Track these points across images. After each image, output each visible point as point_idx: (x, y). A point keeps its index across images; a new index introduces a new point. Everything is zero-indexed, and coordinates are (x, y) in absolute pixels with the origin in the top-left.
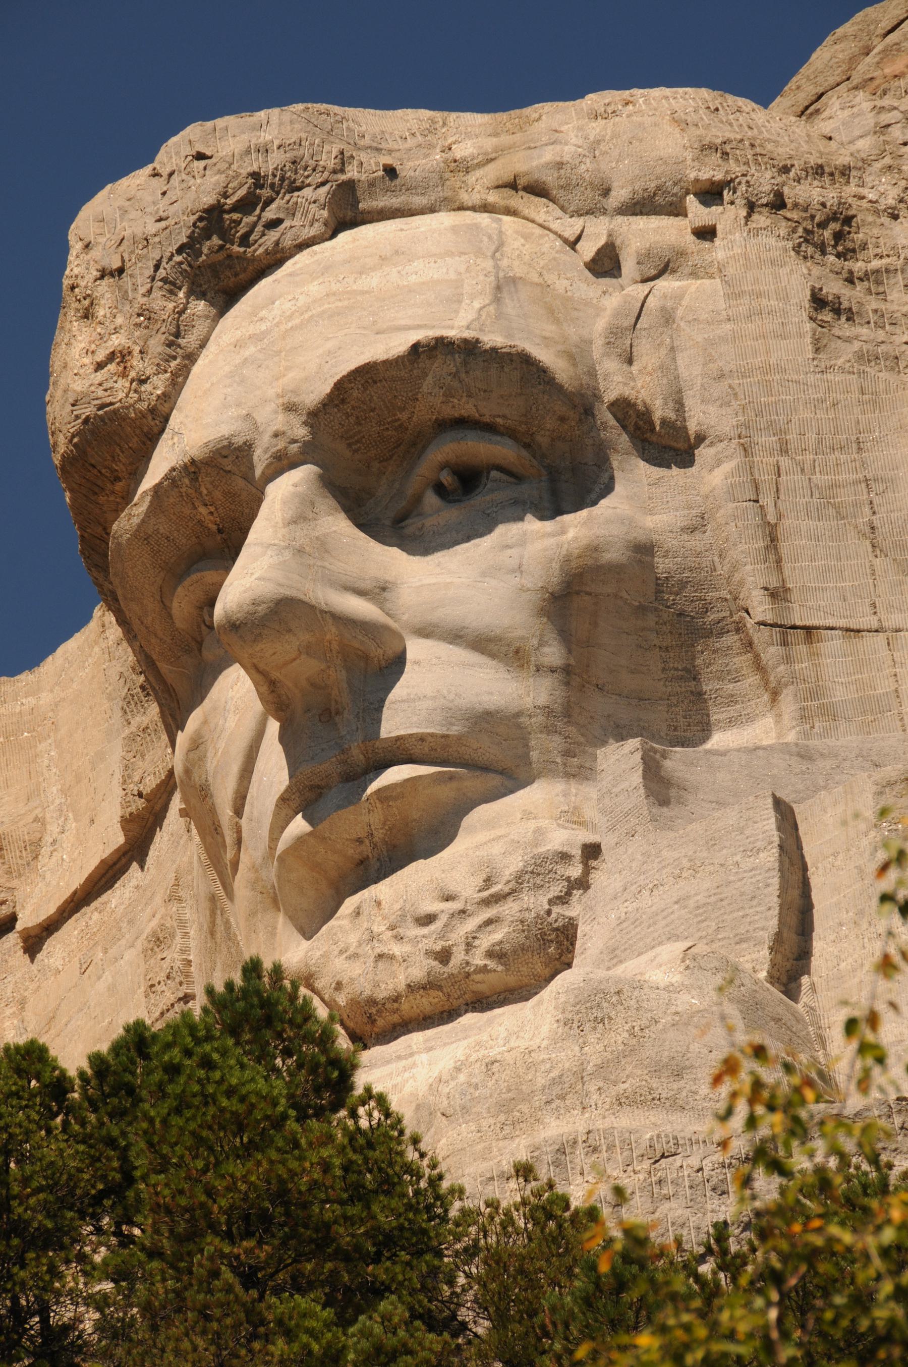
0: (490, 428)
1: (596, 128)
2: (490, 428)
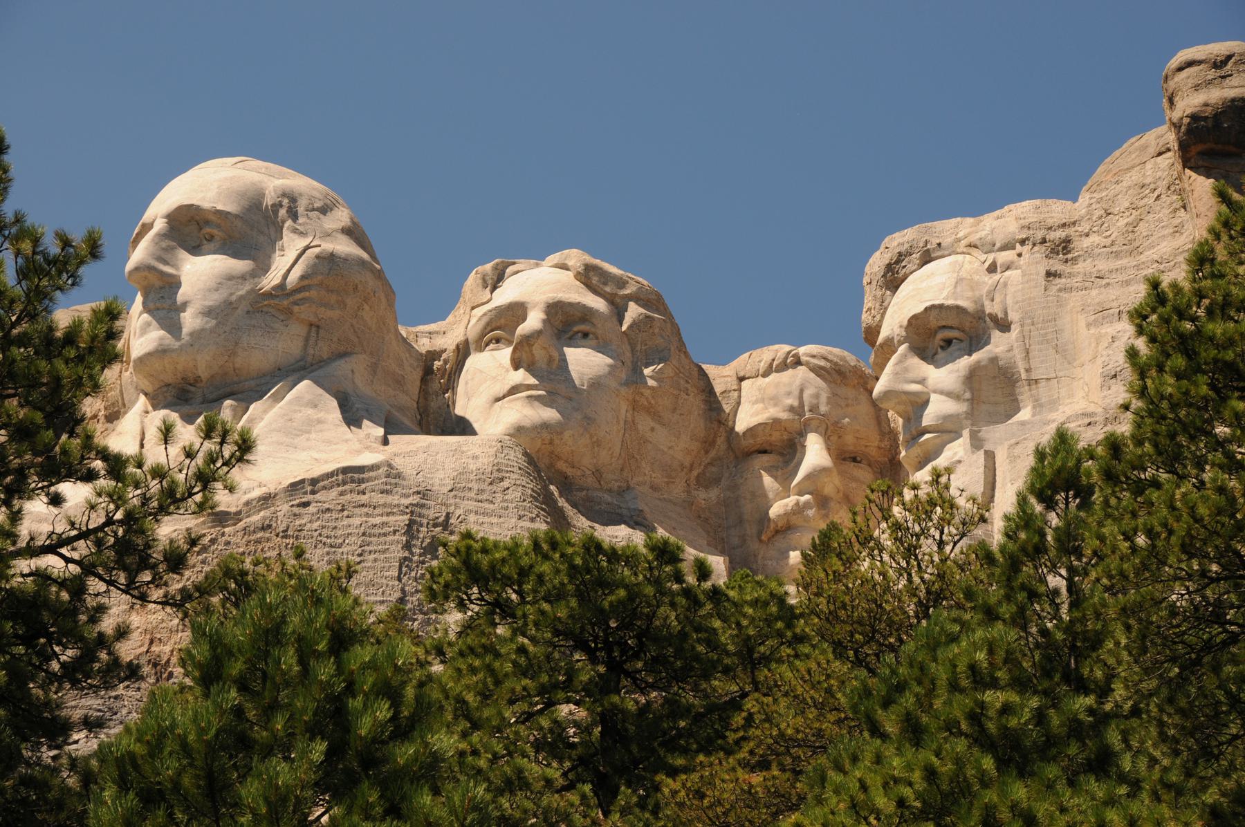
0: (951, 328)
1: (995, 223)
2: (951, 328)
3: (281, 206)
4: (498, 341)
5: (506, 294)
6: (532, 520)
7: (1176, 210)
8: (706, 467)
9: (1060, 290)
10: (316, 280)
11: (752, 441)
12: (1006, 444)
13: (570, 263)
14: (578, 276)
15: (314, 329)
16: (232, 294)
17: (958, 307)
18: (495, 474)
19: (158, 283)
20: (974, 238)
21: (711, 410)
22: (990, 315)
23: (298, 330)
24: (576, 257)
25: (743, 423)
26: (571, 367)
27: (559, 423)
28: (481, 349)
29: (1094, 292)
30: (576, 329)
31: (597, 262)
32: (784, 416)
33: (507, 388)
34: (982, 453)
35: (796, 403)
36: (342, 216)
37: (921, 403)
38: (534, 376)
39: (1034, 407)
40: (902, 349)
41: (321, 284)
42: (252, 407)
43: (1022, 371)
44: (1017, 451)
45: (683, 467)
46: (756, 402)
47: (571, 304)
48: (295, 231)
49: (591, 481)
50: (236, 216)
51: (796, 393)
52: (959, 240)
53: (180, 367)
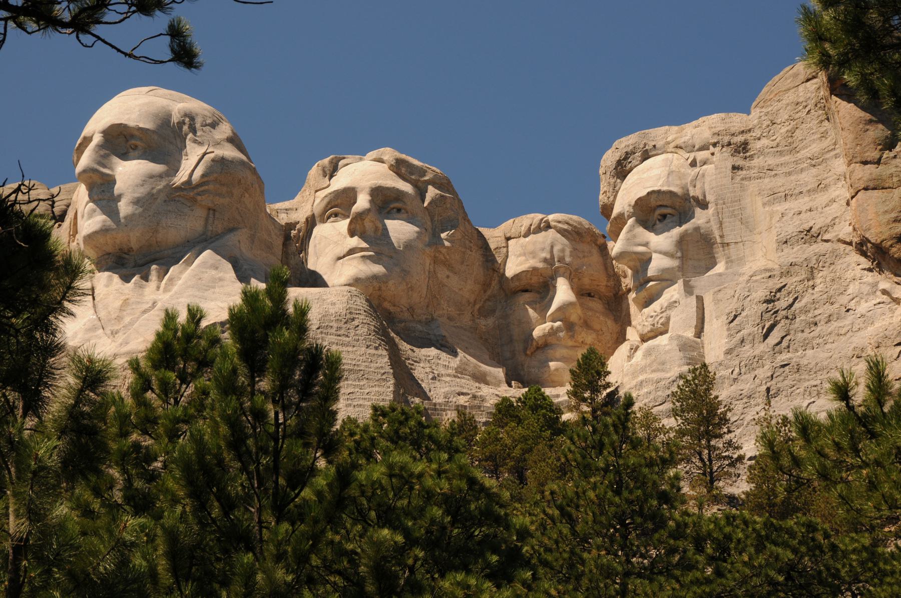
0: (666, 206)
1: (694, 131)
2: (666, 206)
3: (184, 124)
4: (336, 215)
5: (340, 181)
6: (376, 348)
7: (822, 121)
8: (485, 302)
9: (742, 179)
10: (212, 178)
11: (517, 284)
12: (712, 292)
13: (385, 158)
14: (391, 167)
15: (211, 212)
16: (153, 188)
17: (671, 192)
18: (348, 316)
19: (99, 181)
20: (680, 142)
21: (487, 261)
22: (693, 197)
23: (200, 213)
24: (389, 154)
25: (511, 269)
26: (391, 234)
27: (385, 275)
28: (323, 221)
29: (767, 180)
30: (392, 206)
31: (404, 156)
32: (540, 265)
33: (346, 250)
34: (694, 297)
35: (548, 256)
36: (225, 130)
37: (646, 260)
38: (366, 242)
39: (727, 263)
40: (631, 221)
41: (216, 180)
42: (172, 268)
43: (718, 237)
44: (720, 295)
45: (469, 303)
46: (520, 255)
47: (388, 189)
48: (195, 141)
49: (406, 315)
50: (153, 132)
51: (548, 248)
52: (668, 143)
53: (118, 241)
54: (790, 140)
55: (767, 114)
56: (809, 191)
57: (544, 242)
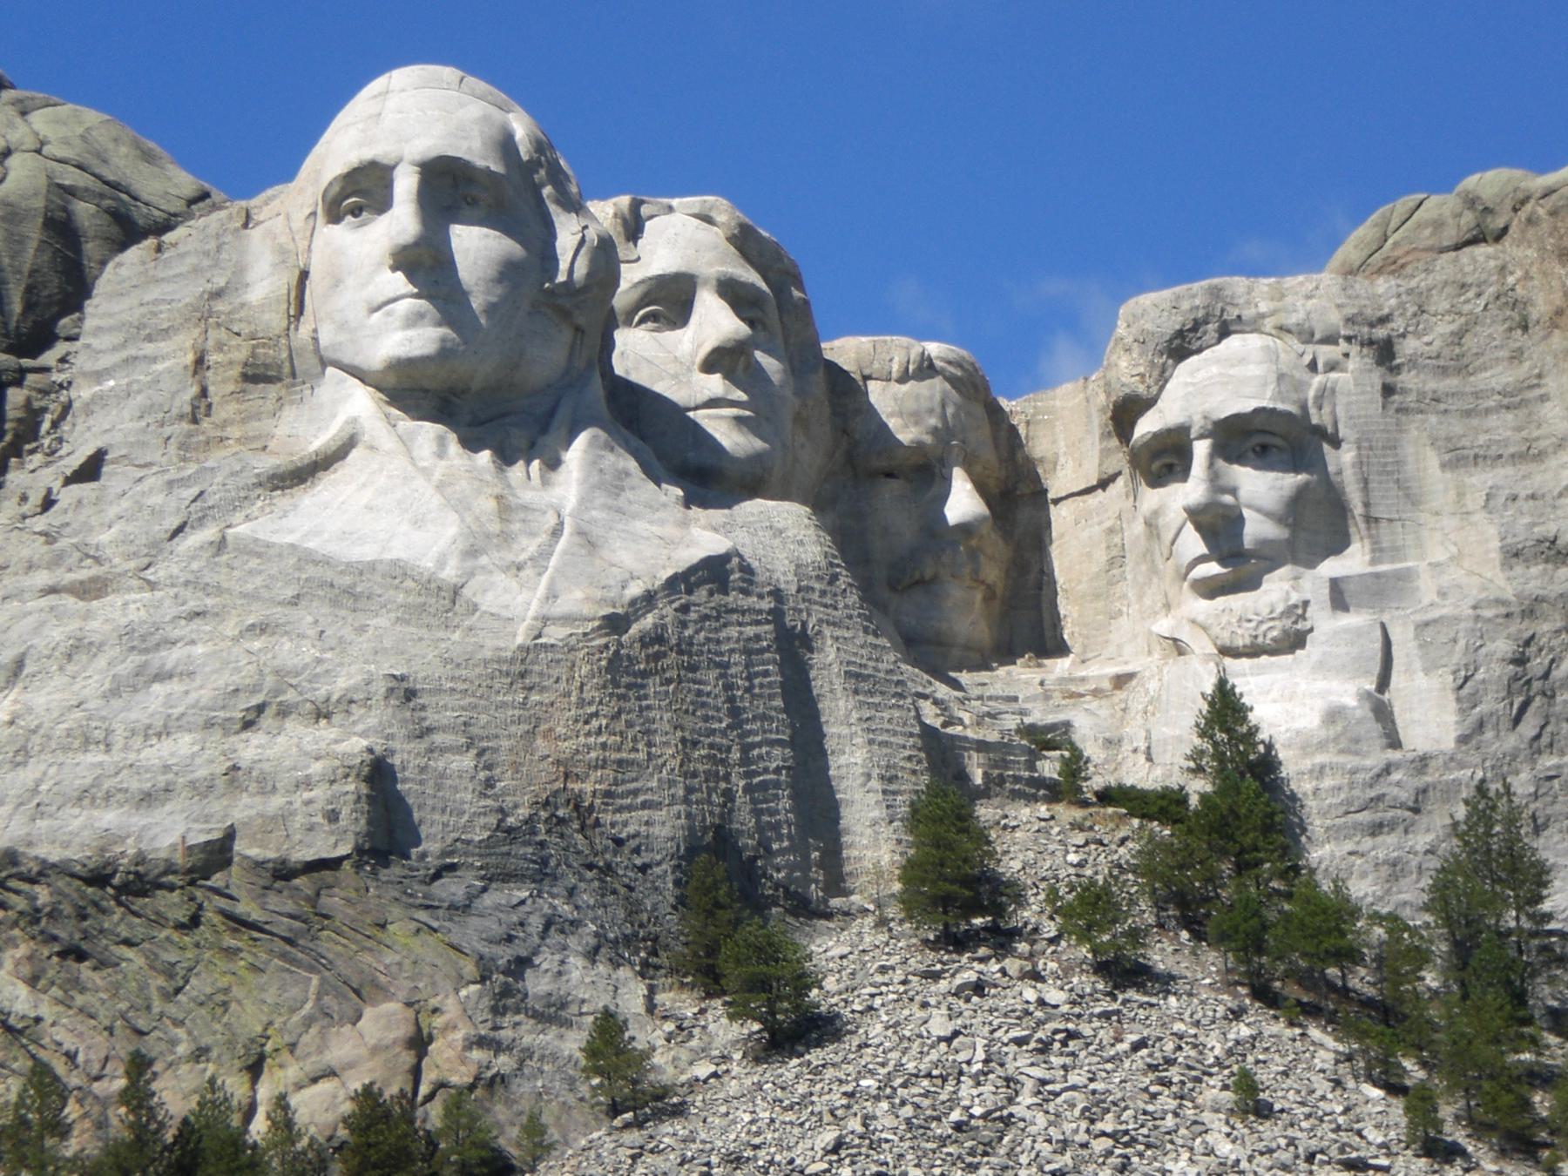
7: (1510, 329)
32: (928, 439)
51: (938, 410)
54: (1457, 350)
55: (1410, 292)
56: (1513, 456)
57: (931, 398)
